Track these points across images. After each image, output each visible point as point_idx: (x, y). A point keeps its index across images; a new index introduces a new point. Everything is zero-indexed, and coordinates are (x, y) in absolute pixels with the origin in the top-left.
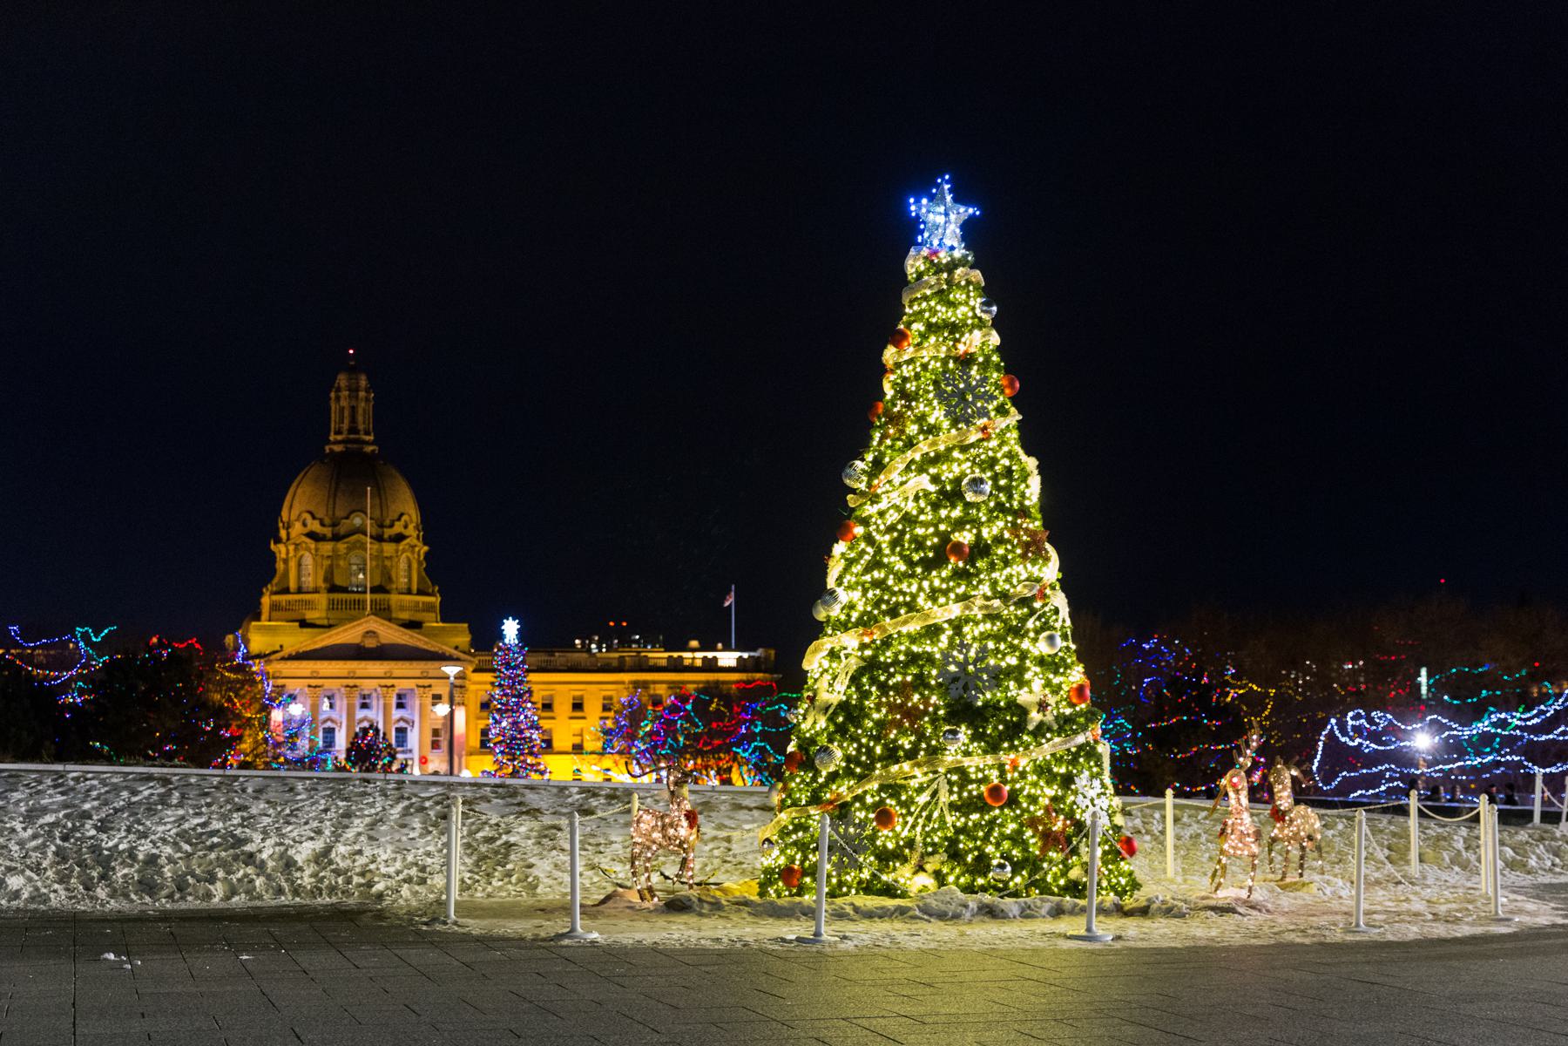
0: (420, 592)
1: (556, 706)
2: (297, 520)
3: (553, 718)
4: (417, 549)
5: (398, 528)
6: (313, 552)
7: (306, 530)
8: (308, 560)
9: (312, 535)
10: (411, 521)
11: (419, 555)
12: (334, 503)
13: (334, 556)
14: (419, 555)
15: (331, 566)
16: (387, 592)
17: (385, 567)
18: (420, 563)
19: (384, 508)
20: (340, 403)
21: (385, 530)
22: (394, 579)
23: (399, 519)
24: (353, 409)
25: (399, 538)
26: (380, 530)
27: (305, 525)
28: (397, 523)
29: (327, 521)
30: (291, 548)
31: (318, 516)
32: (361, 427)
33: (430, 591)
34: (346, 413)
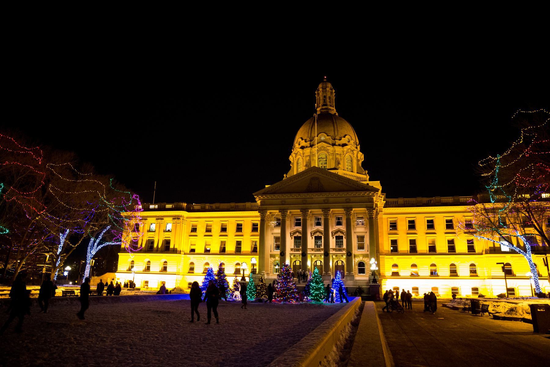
0: (357, 173)
1: (436, 226)
2: (297, 143)
3: (435, 233)
4: (355, 152)
5: (344, 141)
6: (302, 155)
7: (300, 146)
8: (301, 160)
9: (302, 148)
10: (352, 139)
11: (357, 157)
12: (311, 130)
13: (311, 155)
14: (357, 157)
15: (310, 160)
16: (338, 169)
17: (336, 159)
18: (358, 161)
19: (336, 132)
20: (320, 94)
21: (336, 141)
22: (341, 162)
23: (344, 137)
24: (325, 97)
25: (344, 145)
26: (334, 141)
27: (299, 145)
28: (343, 138)
29: (308, 139)
30: (294, 155)
31: (304, 138)
32: (328, 103)
33: (364, 173)
34: (321, 98)
